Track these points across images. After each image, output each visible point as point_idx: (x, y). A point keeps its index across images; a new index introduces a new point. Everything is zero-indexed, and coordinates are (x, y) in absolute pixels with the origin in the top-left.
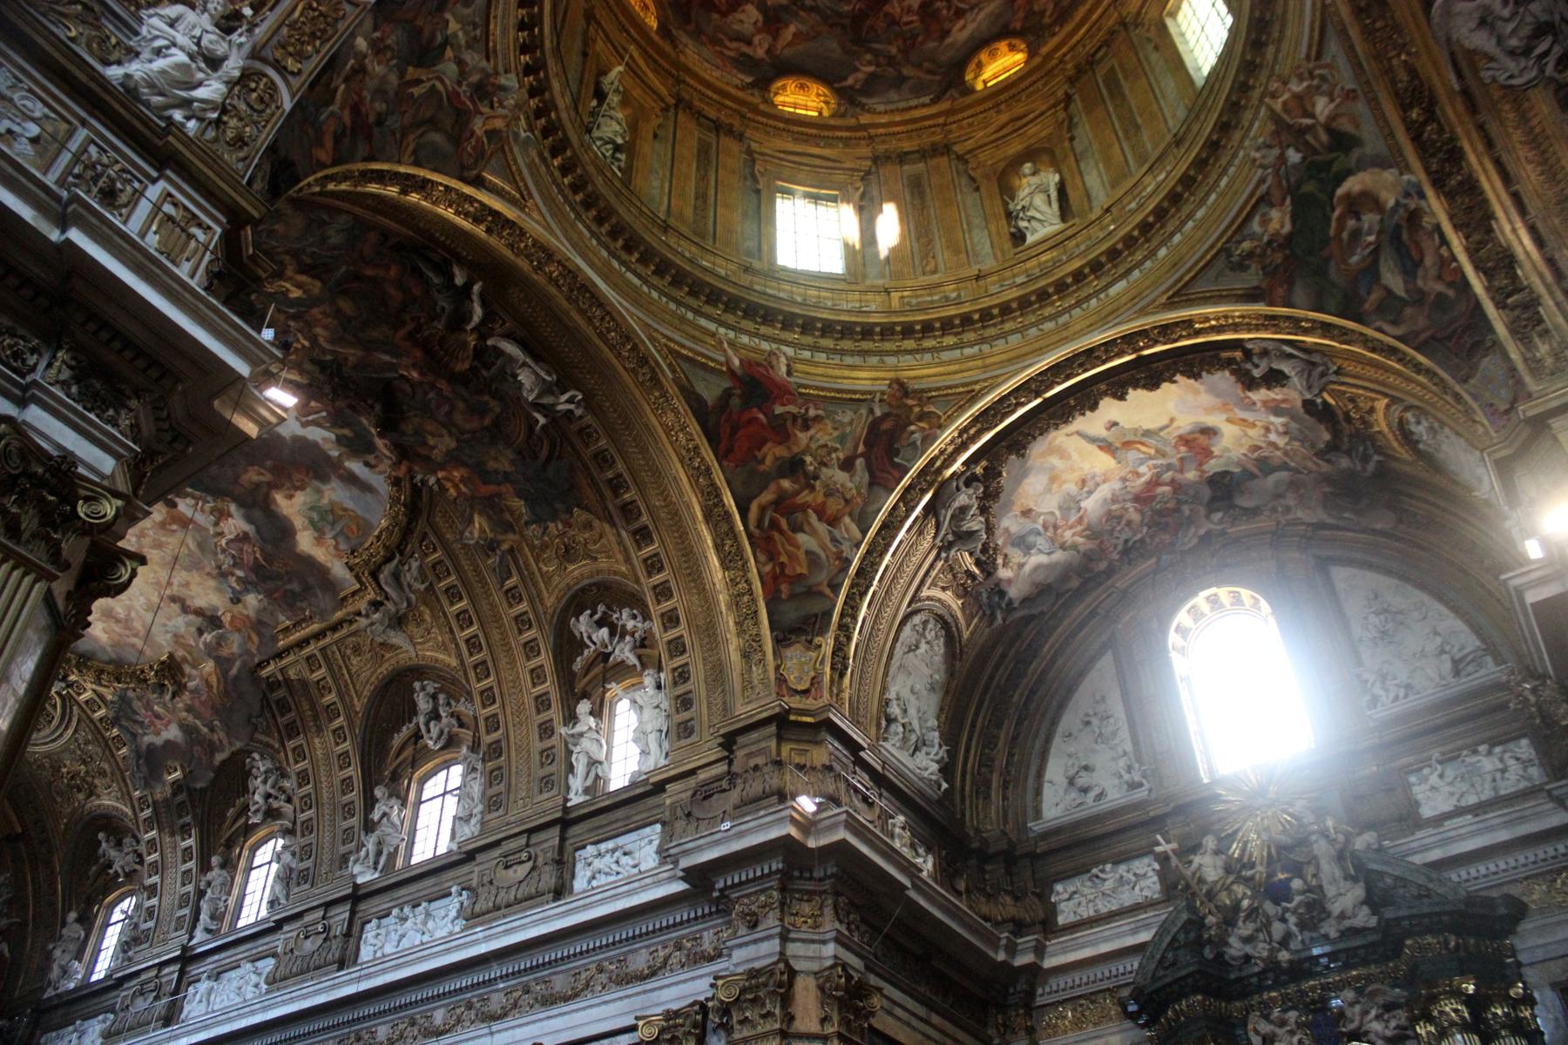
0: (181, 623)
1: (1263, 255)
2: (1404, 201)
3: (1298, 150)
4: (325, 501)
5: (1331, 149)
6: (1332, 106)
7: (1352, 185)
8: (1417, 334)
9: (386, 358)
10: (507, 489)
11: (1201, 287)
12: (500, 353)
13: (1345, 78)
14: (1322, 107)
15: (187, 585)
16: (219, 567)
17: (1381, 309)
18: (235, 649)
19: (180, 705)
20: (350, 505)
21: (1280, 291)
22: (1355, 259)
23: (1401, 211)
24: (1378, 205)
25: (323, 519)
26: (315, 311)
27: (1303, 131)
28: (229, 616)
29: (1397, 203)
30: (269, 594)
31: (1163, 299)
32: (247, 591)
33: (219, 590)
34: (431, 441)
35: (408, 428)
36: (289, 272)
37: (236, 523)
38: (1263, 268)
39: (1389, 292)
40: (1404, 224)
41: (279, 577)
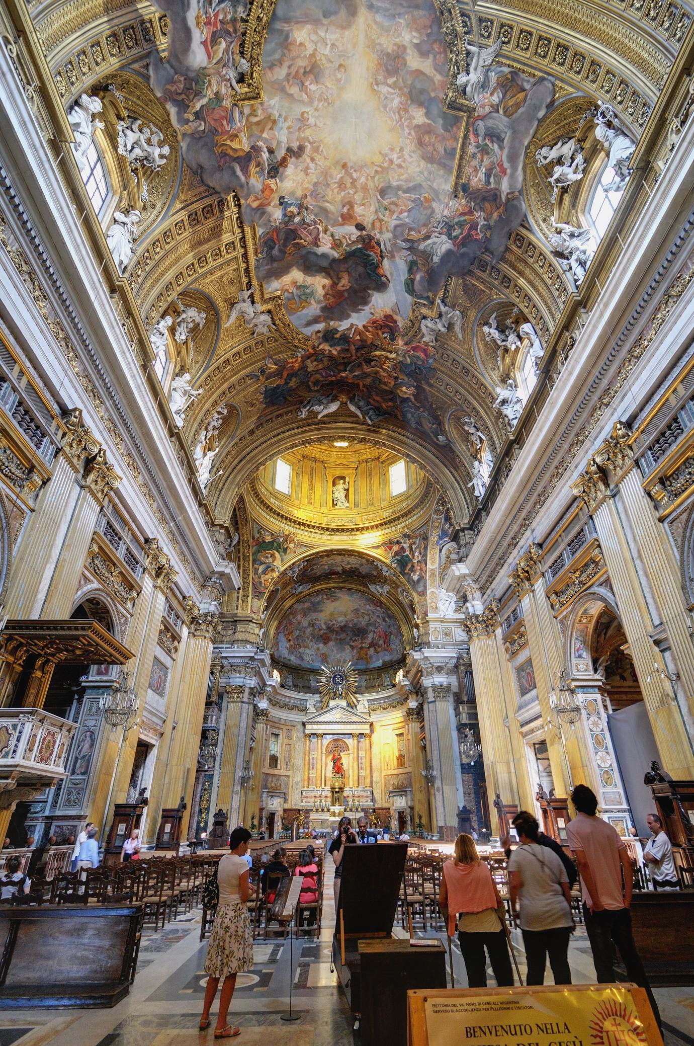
0: (282, 137)
4: (312, 301)
7: (277, 554)
9: (356, 373)
10: (282, 382)
12: (332, 401)
14: (292, 545)
15: (306, 171)
16: (307, 209)
18: (253, 181)
19: (223, 91)
20: (305, 311)
25: (305, 294)
26: (393, 383)
28: (273, 186)
30: (277, 230)
32: (285, 215)
33: (293, 193)
34: (315, 363)
35: (325, 359)
36: (412, 397)
37: (325, 247)
41: (285, 245)
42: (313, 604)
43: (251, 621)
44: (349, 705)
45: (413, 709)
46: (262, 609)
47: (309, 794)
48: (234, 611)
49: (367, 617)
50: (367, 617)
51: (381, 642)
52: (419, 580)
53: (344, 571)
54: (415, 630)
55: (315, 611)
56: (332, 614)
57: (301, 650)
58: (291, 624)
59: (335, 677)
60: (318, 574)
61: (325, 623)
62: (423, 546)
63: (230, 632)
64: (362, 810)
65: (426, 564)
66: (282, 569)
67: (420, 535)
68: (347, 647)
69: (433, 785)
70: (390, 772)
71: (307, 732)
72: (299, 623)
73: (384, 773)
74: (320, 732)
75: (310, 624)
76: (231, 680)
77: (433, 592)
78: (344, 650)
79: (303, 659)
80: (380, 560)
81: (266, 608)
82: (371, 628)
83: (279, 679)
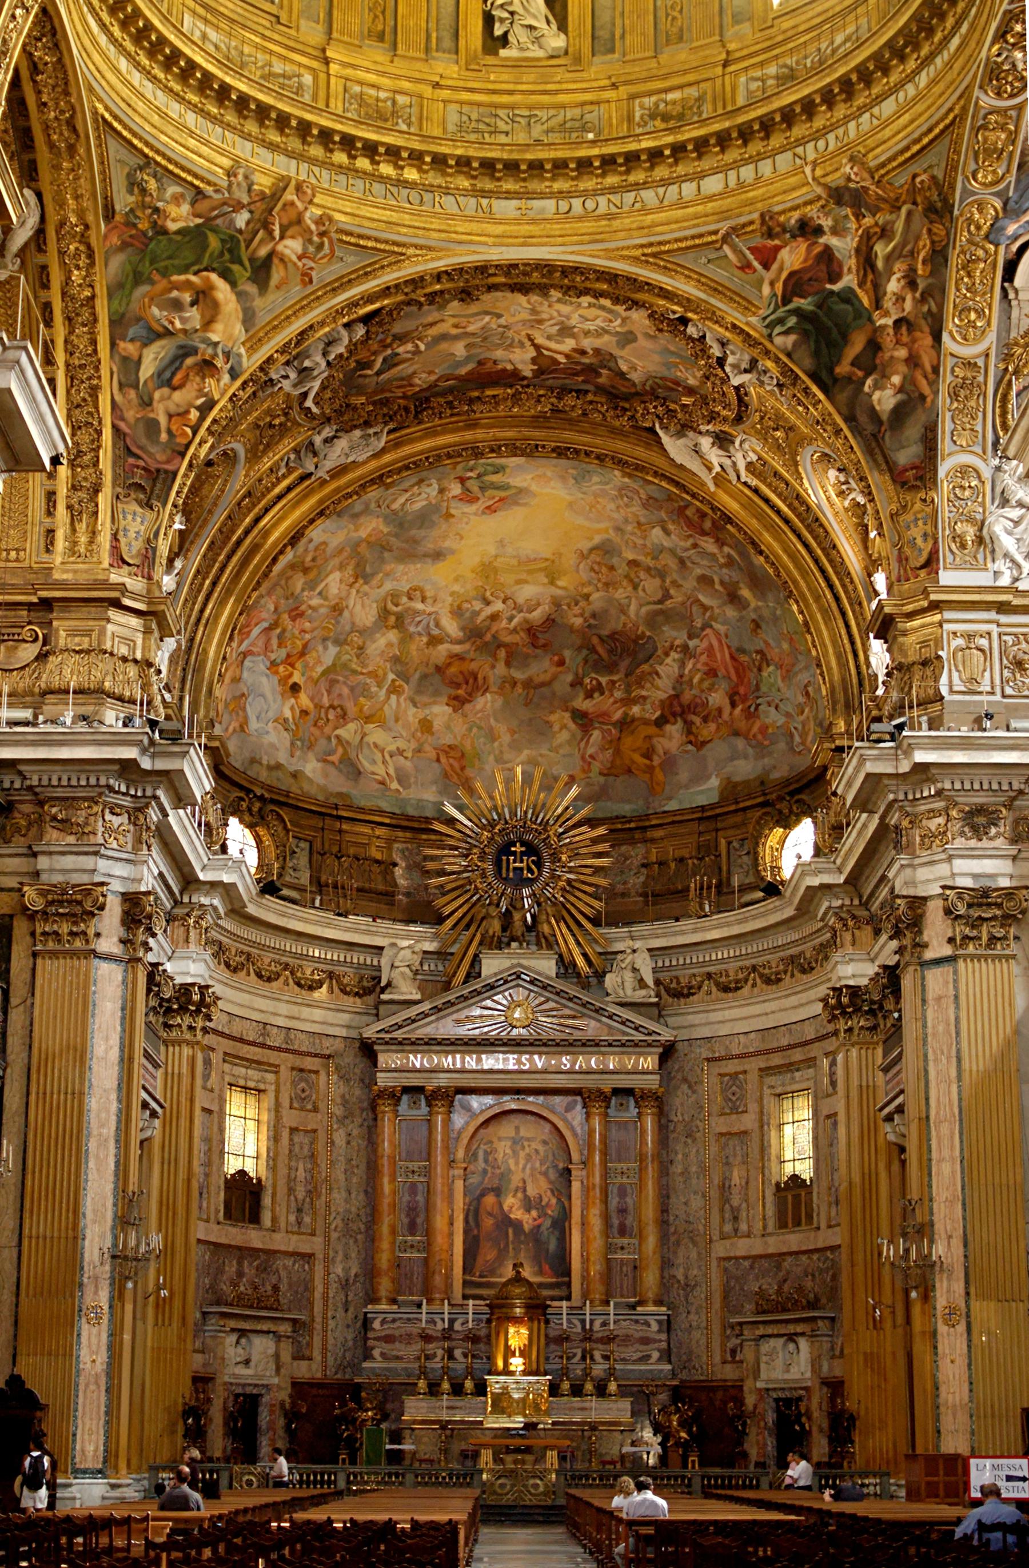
1: (144, 206)
2: (219, 351)
3: (248, 223)
5: (252, 260)
6: (294, 258)
7: (222, 290)
8: (122, 419)
11: (113, 145)
13: (325, 272)
14: (291, 247)
17: (125, 359)
21: (115, 240)
22: (155, 311)
23: (210, 351)
24: (208, 323)
27: (266, 225)
29: (216, 344)
31: (100, 107)
38: (132, 210)
39: (139, 362)
40: (199, 357)
42: (399, 522)
43: (116, 604)
44: (566, 967)
45: (855, 991)
46: (163, 548)
47: (398, 1329)
48: (33, 554)
49: (651, 586)
50: (651, 586)
51: (717, 698)
52: (900, 413)
53: (544, 366)
54: (877, 646)
55: (410, 553)
56: (487, 570)
57: (348, 732)
58: (296, 614)
59: (505, 850)
60: (421, 380)
61: (457, 612)
62: (925, 241)
63: (28, 652)
64: (623, 1391)
65: (937, 338)
66: (250, 364)
67: (913, 190)
68: (560, 718)
69: (927, 1296)
70: (742, 1247)
71: (383, 1080)
72: (337, 610)
73: (720, 1249)
74: (442, 1081)
75: (384, 613)
76: (43, 862)
77: (964, 471)
78: (541, 731)
79: (355, 772)
80: (713, 316)
81: (183, 543)
82: (673, 634)
83: (252, 858)
